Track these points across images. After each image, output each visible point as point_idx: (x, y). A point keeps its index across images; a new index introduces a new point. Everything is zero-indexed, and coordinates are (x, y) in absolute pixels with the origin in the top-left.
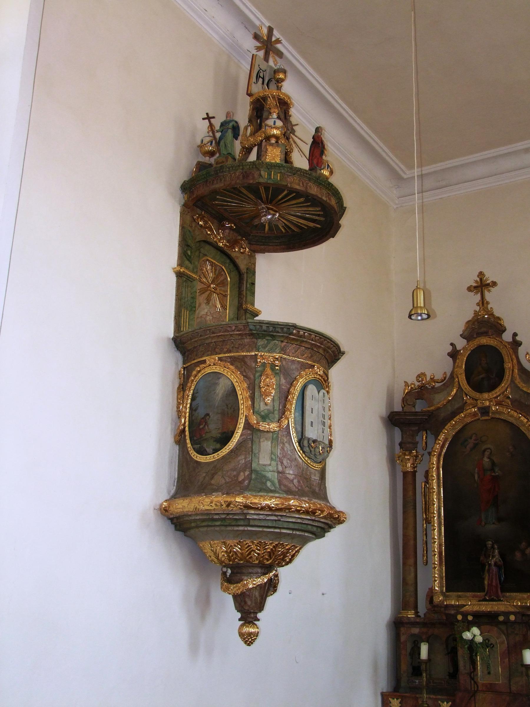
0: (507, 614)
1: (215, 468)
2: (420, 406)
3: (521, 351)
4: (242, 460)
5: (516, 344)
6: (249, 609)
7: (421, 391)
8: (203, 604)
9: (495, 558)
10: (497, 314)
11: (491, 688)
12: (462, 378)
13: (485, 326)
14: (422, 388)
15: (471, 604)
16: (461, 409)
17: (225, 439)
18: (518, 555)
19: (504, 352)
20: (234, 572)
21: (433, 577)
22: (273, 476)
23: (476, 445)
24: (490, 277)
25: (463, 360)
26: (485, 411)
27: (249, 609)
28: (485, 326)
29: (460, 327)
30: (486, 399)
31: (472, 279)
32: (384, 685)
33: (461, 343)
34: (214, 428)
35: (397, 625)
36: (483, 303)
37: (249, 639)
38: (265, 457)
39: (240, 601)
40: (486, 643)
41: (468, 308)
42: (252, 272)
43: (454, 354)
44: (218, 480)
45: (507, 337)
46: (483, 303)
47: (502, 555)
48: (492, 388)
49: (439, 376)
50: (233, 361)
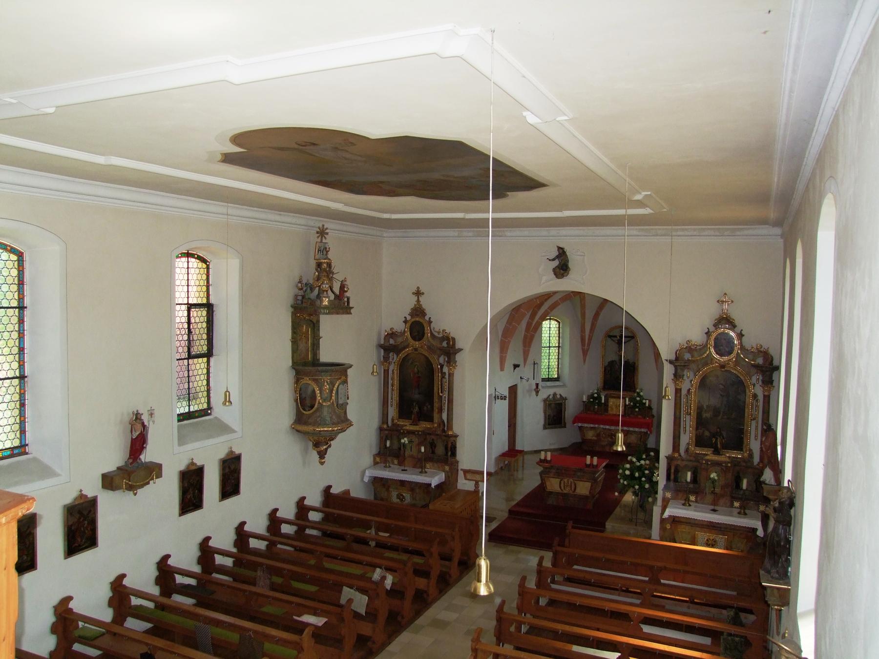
0: (418, 431)
1: (310, 416)
2: (392, 341)
3: (432, 325)
4: (318, 414)
5: (430, 322)
6: (322, 455)
7: (392, 335)
8: (306, 450)
9: (416, 409)
10: (424, 307)
11: (412, 457)
12: (408, 334)
13: (418, 311)
14: (392, 333)
15: (407, 425)
16: (407, 346)
17: (312, 407)
18: (425, 408)
19: (425, 325)
20: (316, 445)
21: (392, 412)
22: (328, 419)
23: (412, 363)
24: (422, 290)
25: (408, 325)
26: (416, 350)
27: (322, 455)
28: (418, 311)
29: (409, 311)
30: (417, 344)
31: (414, 290)
32: (375, 451)
33: (409, 318)
34: (308, 402)
35: (381, 429)
36: (418, 301)
37: (322, 463)
38: (326, 413)
39: (319, 453)
40: (410, 442)
41: (412, 301)
42: (318, 321)
43: (405, 322)
44: (310, 421)
45: (427, 318)
46: (418, 301)
47: (419, 408)
48: (420, 340)
49: (399, 331)
50: (314, 380)
